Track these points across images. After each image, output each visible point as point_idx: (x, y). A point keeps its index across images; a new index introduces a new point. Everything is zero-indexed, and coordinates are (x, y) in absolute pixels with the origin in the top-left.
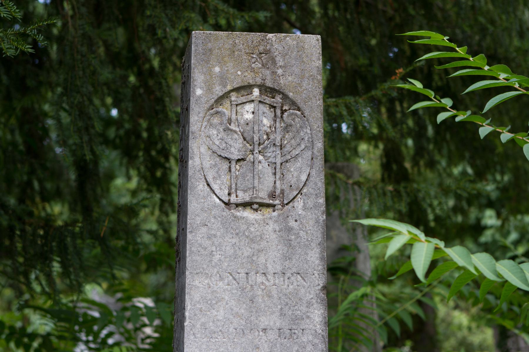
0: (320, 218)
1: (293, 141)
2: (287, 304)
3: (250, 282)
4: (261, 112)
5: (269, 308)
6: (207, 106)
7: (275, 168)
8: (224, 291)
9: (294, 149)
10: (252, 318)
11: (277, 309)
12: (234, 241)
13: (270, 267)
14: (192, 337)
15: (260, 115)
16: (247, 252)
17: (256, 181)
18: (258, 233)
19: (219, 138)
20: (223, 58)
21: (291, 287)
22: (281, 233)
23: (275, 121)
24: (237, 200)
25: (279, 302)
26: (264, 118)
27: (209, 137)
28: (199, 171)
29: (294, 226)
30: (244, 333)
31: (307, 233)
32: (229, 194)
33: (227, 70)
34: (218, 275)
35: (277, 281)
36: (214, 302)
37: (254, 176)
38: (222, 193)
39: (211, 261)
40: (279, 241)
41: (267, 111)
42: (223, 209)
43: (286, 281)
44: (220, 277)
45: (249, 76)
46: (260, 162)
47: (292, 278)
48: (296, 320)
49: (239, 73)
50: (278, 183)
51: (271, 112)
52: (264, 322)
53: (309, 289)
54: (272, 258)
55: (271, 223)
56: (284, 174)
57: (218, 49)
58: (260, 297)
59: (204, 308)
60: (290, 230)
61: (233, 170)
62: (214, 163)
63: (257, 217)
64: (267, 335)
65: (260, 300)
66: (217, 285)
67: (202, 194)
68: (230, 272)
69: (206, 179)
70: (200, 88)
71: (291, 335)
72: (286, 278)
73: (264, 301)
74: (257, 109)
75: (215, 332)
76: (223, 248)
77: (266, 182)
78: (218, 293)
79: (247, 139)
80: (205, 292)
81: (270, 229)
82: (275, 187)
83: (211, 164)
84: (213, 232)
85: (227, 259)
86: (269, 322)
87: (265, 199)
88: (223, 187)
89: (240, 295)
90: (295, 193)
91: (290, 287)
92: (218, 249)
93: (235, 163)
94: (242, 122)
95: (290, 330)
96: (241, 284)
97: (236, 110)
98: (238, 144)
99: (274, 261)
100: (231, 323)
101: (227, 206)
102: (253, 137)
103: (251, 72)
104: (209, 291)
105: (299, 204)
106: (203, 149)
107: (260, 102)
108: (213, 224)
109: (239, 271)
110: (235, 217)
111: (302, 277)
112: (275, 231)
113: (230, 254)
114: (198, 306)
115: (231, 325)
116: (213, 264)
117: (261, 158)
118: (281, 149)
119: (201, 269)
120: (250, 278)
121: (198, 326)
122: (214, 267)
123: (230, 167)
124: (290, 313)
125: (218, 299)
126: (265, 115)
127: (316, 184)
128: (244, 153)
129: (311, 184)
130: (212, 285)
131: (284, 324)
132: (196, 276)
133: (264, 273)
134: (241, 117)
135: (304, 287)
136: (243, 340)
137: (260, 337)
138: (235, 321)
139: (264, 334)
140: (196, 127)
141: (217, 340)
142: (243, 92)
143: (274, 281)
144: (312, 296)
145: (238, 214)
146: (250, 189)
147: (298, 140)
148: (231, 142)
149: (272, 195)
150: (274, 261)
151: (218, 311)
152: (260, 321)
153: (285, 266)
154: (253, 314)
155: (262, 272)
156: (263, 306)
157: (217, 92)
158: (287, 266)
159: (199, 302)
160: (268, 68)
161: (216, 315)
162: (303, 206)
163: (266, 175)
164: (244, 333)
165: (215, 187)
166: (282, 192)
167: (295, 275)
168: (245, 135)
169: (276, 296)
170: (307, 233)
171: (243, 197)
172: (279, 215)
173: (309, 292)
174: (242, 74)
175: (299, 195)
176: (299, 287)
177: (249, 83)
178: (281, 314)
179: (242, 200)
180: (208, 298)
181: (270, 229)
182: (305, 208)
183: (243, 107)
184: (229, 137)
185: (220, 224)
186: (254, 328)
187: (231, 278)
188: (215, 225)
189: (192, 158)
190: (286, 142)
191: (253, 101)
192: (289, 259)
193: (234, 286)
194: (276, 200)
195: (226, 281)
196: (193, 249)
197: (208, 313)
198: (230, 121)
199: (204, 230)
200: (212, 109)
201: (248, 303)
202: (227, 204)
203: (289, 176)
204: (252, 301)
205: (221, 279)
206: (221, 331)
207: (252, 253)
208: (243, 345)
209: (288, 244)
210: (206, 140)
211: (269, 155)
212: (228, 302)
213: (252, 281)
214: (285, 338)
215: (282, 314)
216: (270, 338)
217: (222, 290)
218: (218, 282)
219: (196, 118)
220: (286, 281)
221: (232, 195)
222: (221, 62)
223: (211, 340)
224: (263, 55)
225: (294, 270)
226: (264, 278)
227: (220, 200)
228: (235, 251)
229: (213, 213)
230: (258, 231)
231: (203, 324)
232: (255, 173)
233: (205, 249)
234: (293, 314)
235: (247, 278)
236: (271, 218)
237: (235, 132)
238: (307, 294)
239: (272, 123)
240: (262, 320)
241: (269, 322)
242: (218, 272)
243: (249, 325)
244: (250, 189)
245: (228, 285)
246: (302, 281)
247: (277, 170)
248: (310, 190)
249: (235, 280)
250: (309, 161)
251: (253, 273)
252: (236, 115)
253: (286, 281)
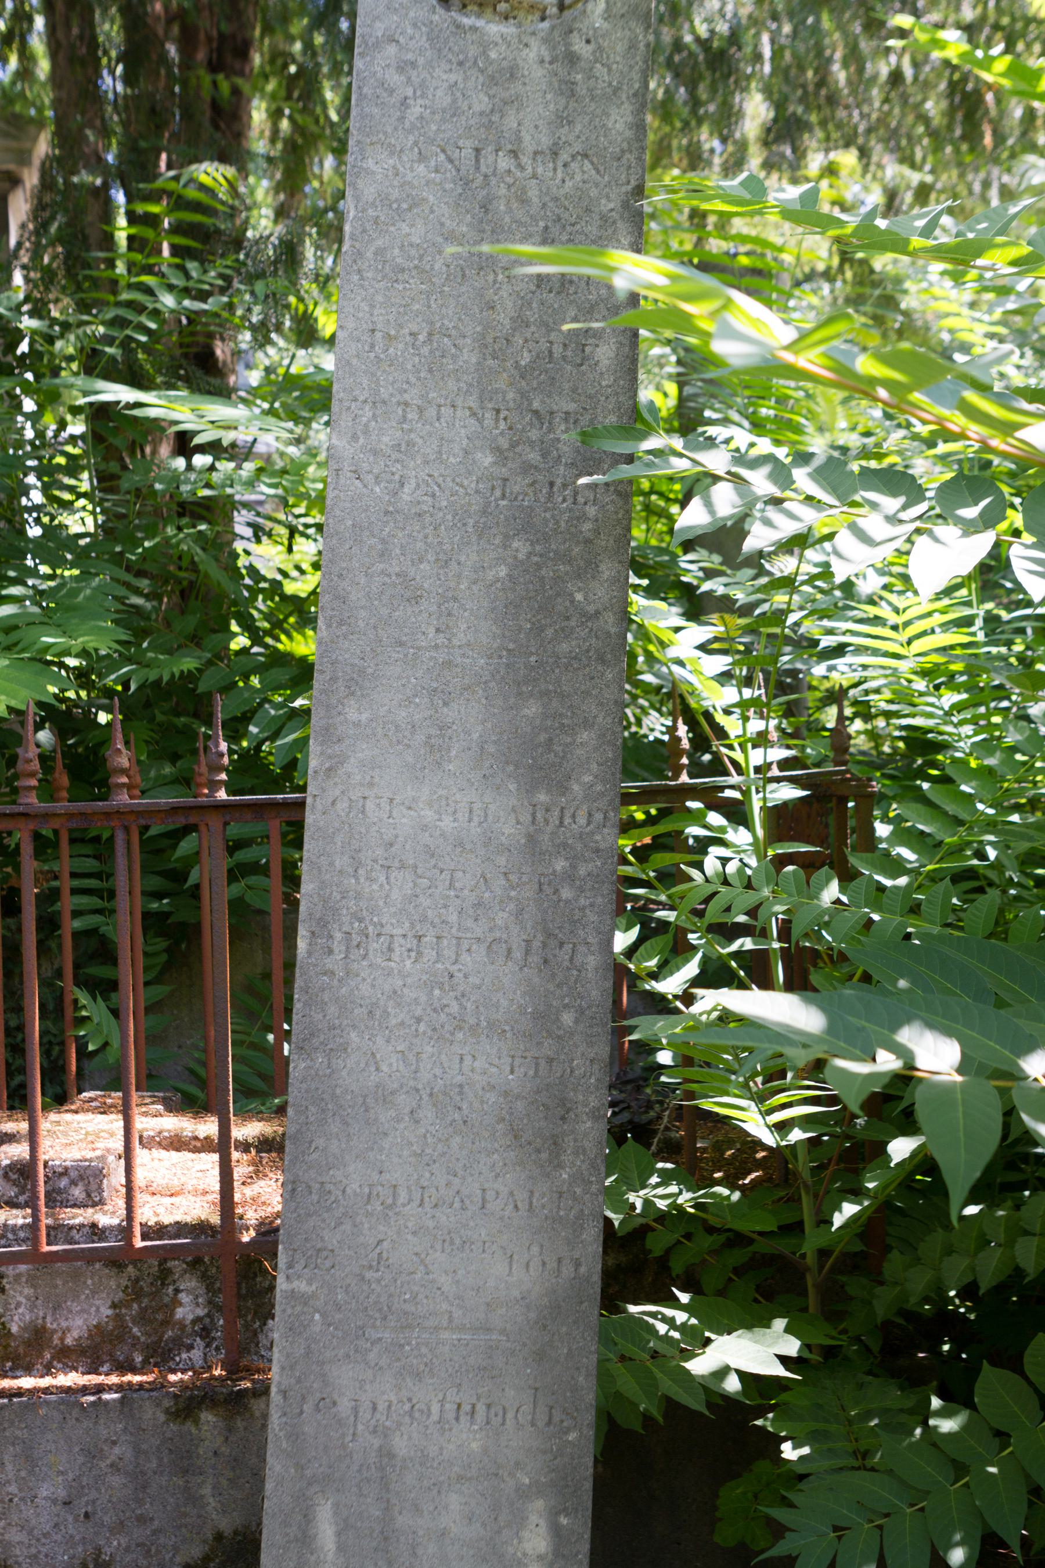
3: (483, 169)
8: (428, 183)
12: (453, 77)
13: (527, 138)
14: (356, 277)
16: (481, 102)
18: (505, 64)
21: (569, 184)
30: (464, 276)
31: (610, 70)
35: (540, 170)
36: (405, 206)
39: (401, 119)
40: (550, 83)
54: (533, 120)
55: (534, 43)
58: (503, 202)
60: (572, 59)
72: (560, 164)
75: (403, 270)
78: (413, 187)
85: (437, 117)
109: (461, 143)
112: (542, 61)
114: (371, 212)
116: (407, 124)
122: (410, 132)
135: (597, 185)
136: (464, 289)
144: (611, 205)
145: (466, 21)
155: (509, 147)
156: (507, 219)
159: (373, 205)
164: (464, 276)
169: (535, 200)
170: (610, 70)
172: (553, 28)
173: (608, 197)
180: (393, 198)
181: (532, 55)
187: (442, 157)
192: (569, 123)
195: (433, 163)
196: (365, 90)
199: (392, 50)
204: (485, 207)
205: (422, 158)
209: (568, 89)
225: (578, 147)
228: (454, 101)
229: (412, 14)
231: (379, 252)
233: (391, 92)
235: (477, 161)
236: (534, 34)
242: (416, 143)
245: (437, 171)
249: (451, 161)
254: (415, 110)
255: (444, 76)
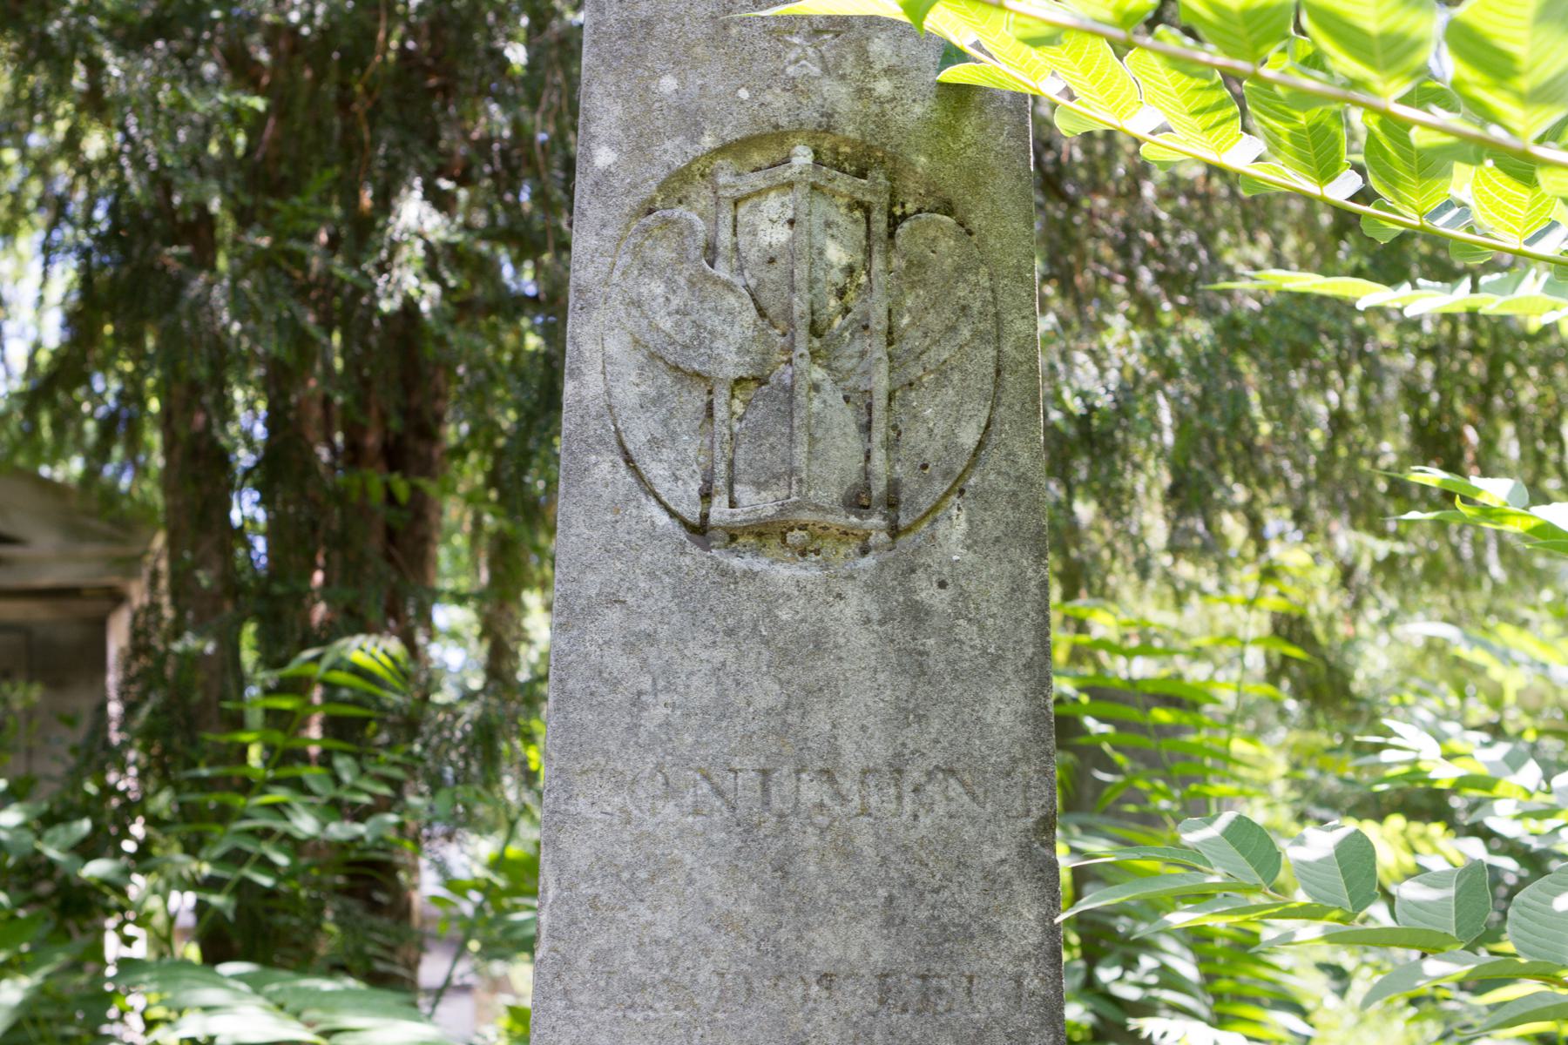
0: (1030, 573)
1: (930, 318)
2: (912, 883)
3: (776, 804)
4: (817, 221)
5: (845, 894)
6: (631, 202)
7: (869, 407)
8: (681, 833)
9: (936, 342)
10: (783, 935)
11: (873, 902)
12: (718, 655)
13: (847, 747)
14: (561, 1004)
15: (816, 231)
16: (767, 693)
17: (801, 452)
18: (804, 628)
19: (673, 307)
20: (688, 48)
21: (925, 820)
22: (888, 627)
23: (868, 252)
24: (733, 515)
25: (882, 873)
26: (829, 242)
27: (637, 303)
28: (600, 416)
29: (935, 601)
30: (750, 991)
31: (982, 628)
32: (706, 496)
33: (702, 87)
34: (660, 778)
35: (874, 801)
36: (643, 875)
37: (791, 434)
38: (679, 492)
39: (633, 728)
40: (883, 655)
41: (840, 220)
42: (683, 544)
43: (908, 799)
44: (667, 783)
45: (776, 105)
46: (816, 387)
47: (929, 788)
48: (945, 938)
49: (744, 94)
50: (879, 456)
51: (856, 221)
52: (825, 949)
53: (992, 827)
54: (857, 719)
55: (853, 592)
56: (901, 427)
57: (671, 20)
58: (812, 858)
59: (605, 898)
60: (917, 614)
61: (721, 413)
62: (653, 393)
63: (802, 574)
64: (839, 995)
65: (812, 868)
66: (654, 815)
67: (606, 494)
68: (704, 765)
69: (621, 444)
70: (611, 145)
71: (925, 997)
72: (907, 789)
73: (826, 873)
74: (804, 208)
75: (643, 987)
76: (680, 684)
77: (833, 453)
78: (656, 841)
79: (771, 312)
80: (612, 838)
81: (849, 612)
82: (867, 474)
83: (644, 394)
84: (643, 626)
85: (693, 721)
86: (846, 947)
87: (832, 511)
88: (684, 473)
89: (739, 850)
90: (940, 487)
91: (921, 818)
92: (661, 683)
93: (728, 393)
94: (753, 255)
95: (924, 978)
96: (742, 811)
97: (735, 218)
98: (737, 328)
99: (863, 728)
100: (706, 952)
101: (696, 537)
102: (790, 307)
103: (784, 90)
104: (626, 836)
105: (955, 527)
106: (614, 346)
107: (814, 187)
108: (646, 597)
109: (735, 764)
110: (724, 573)
111: (963, 783)
112: (868, 621)
113: (705, 701)
114: (584, 888)
115: (703, 960)
116: (643, 737)
117: (818, 374)
118: (890, 343)
119: (599, 758)
120: (774, 790)
121: (581, 962)
122: (648, 748)
123: (710, 407)
124: (923, 914)
125: (656, 862)
126: (835, 231)
127: (1011, 457)
128: (758, 358)
129: (994, 457)
130: (636, 812)
131: (899, 953)
132: (579, 781)
133: (827, 772)
134: (749, 238)
135: (973, 820)
136: (751, 1014)
137: (810, 1005)
138: (720, 942)
139: (825, 994)
140: (591, 270)
141: (652, 1014)
142: (757, 158)
143: (862, 798)
144: (1002, 854)
145: (736, 563)
146: (777, 477)
147: (948, 314)
148: (715, 322)
149: (857, 501)
150: (863, 728)
151: (657, 908)
152: (810, 946)
153: (904, 745)
154: (784, 919)
155: (820, 764)
156: (822, 888)
157: (666, 158)
158: (911, 746)
159: (589, 877)
160: (843, 77)
161: (651, 924)
162: (968, 535)
163: (836, 431)
164: (750, 991)
165: (656, 471)
166: (894, 486)
167: (940, 776)
168: (766, 297)
169: (869, 852)
170: (982, 628)
171: (755, 503)
172: (882, 566)
173: (994, 840)
174: (753, 97)
175: (954, 498)
176: (957, 822)
177: (777, 126)
178: (888, 922)
179: (752, 516)
180: (622, 862)
181: (849, 612)
182: (972, 541)
183: (756, 206)
184: (706, 306)
185: (668, 595)
186: (791, 972)
187: (705, 787)
188: (651, 601)
189: (577, 374)
190: (906, 320)
191: (791, 185)
192: (919, 718)
193: (717, 817)
194: (870, 516)
195: (689, 799)
196: (571, 684)
197: (622, 915)
198: (711, 251)
199: (614, 616)
200: (651, 211)
201: (768, 877)
202: (700, 530)
203: (915, 436)
204: (782, 870)
205: (671, 791)
206: (665, 980)
207: (784, 698)
208: (748, 1034)
209: (915, 665)
210: (629, 315)
211: (849, 365)
212: (695, 875)
213: (783, 799)
214: (904, 1010)
215: (892, 920)
216: (847, 1009)
217: (674, 831)
218: (660, 804)
219: (593, 241)
220: (907, 800)
221: (716, 500)
222: (680, 61)
223: (630, 1014)
224: (826, 37)
225: (936, 758)
226: (826, 786)
227: (673, 514)
228: (722, 693)
229: (646, 558)
230: (803, 620)
232: (797, 422)
233: (615, 684)
234: (933, 918)
235: (766, 790)
236: (851, 577)
237: (729, 287)
238: (986, 848)
239: (860, 257)
240: (820, 943)
241: (846, 947)
242: (659, 767)
243: (770, 959)
244: (777, 477)
245: (696, 812)
246: (966, 798)
247: (876, 414)
248: (992, 477)
249: (720, 793)
250: (988, 380)
251: (785, 770)
252: (735, 234)
253: (908, 799)
254: (657, 713)
255: (704, 654)
